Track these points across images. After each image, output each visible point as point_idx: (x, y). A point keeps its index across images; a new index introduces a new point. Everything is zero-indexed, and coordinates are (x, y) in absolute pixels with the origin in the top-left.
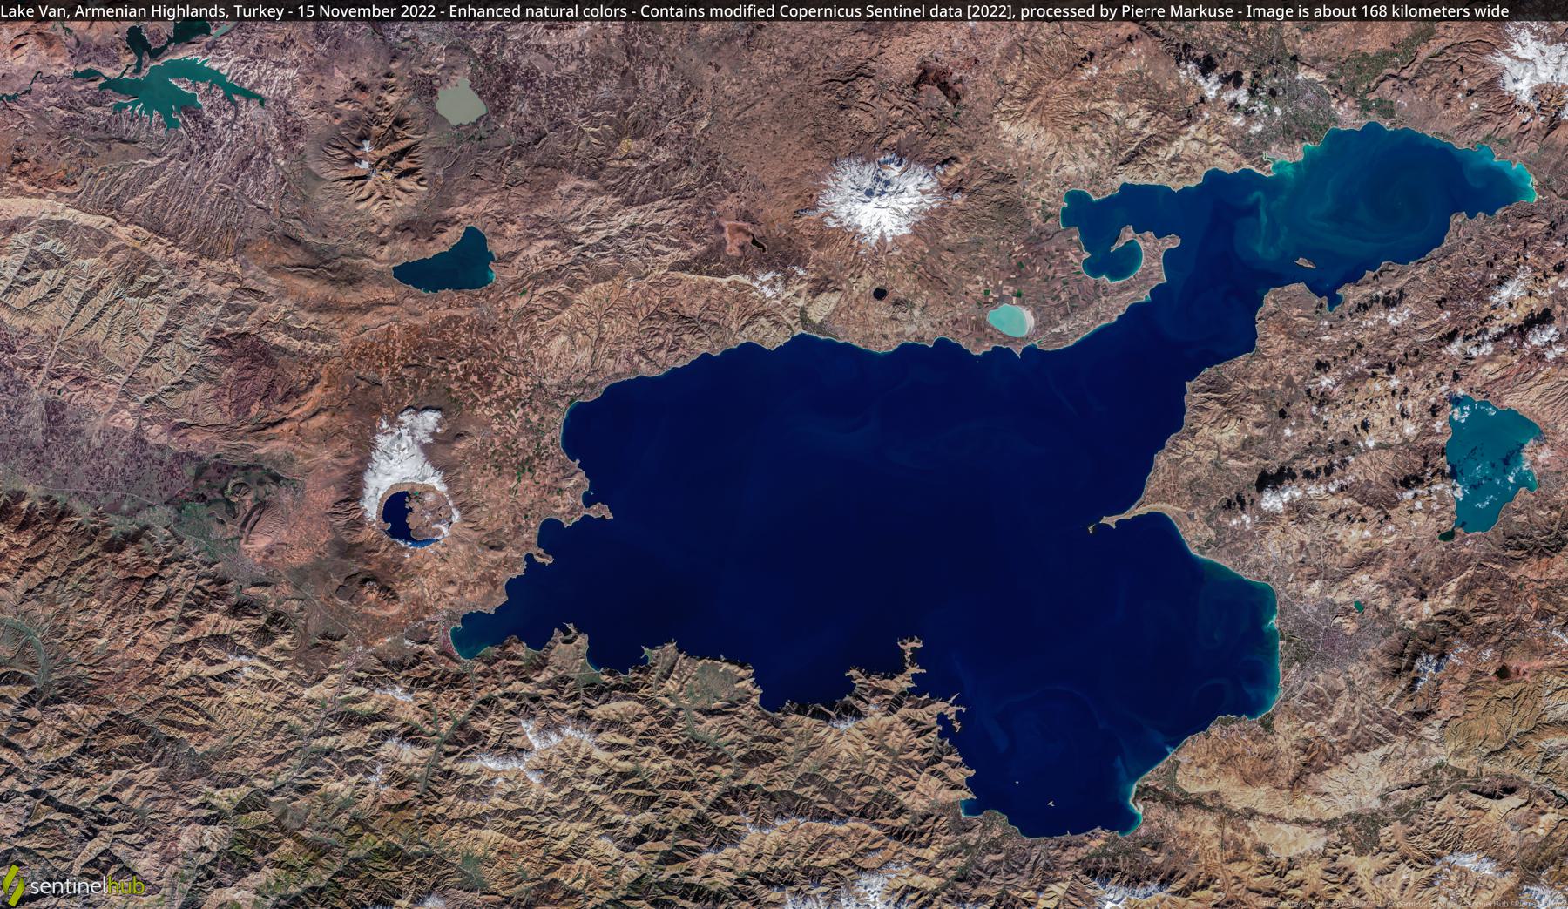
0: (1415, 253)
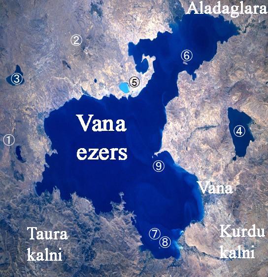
0: (209, 59)
